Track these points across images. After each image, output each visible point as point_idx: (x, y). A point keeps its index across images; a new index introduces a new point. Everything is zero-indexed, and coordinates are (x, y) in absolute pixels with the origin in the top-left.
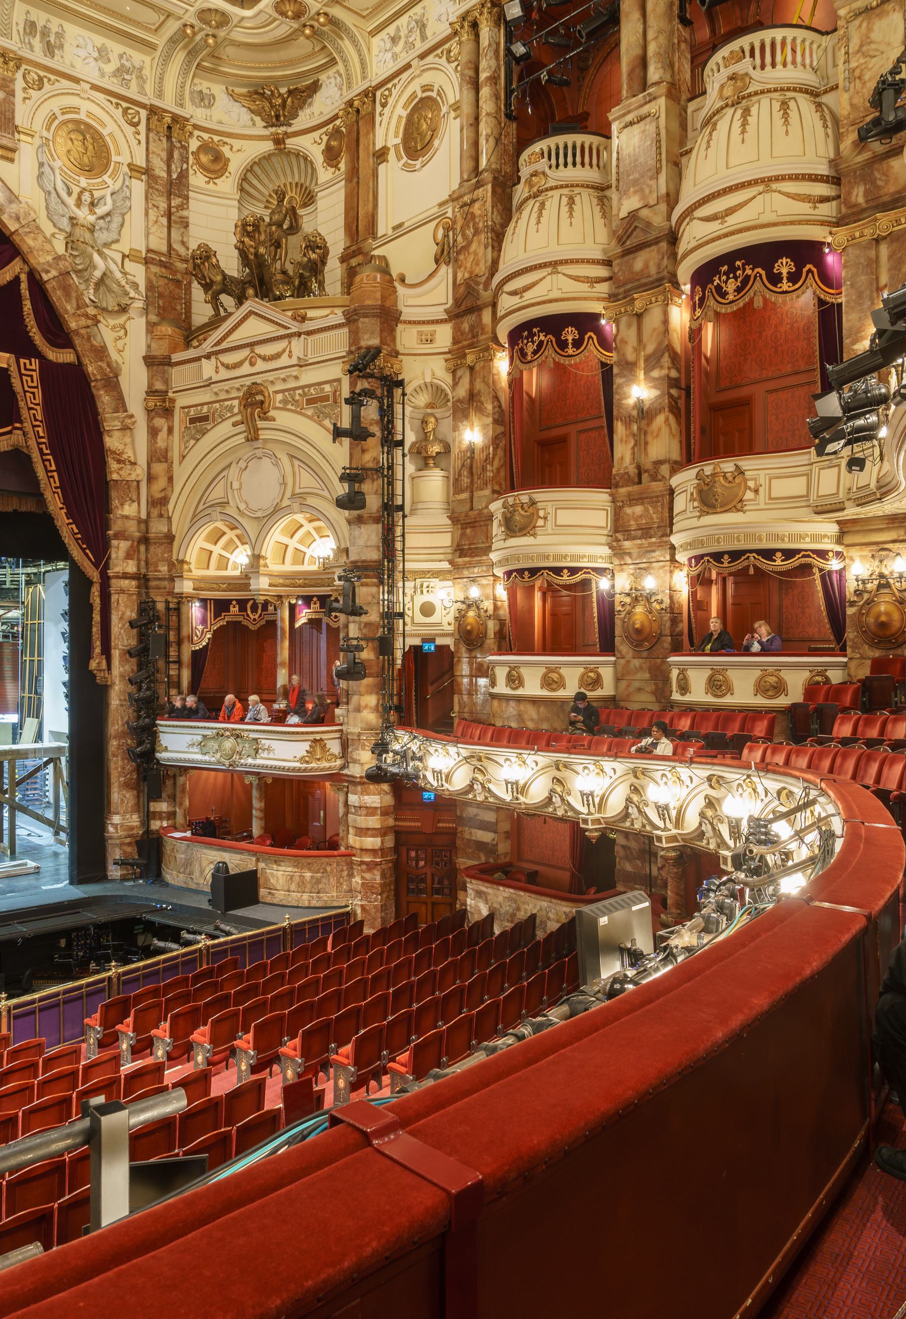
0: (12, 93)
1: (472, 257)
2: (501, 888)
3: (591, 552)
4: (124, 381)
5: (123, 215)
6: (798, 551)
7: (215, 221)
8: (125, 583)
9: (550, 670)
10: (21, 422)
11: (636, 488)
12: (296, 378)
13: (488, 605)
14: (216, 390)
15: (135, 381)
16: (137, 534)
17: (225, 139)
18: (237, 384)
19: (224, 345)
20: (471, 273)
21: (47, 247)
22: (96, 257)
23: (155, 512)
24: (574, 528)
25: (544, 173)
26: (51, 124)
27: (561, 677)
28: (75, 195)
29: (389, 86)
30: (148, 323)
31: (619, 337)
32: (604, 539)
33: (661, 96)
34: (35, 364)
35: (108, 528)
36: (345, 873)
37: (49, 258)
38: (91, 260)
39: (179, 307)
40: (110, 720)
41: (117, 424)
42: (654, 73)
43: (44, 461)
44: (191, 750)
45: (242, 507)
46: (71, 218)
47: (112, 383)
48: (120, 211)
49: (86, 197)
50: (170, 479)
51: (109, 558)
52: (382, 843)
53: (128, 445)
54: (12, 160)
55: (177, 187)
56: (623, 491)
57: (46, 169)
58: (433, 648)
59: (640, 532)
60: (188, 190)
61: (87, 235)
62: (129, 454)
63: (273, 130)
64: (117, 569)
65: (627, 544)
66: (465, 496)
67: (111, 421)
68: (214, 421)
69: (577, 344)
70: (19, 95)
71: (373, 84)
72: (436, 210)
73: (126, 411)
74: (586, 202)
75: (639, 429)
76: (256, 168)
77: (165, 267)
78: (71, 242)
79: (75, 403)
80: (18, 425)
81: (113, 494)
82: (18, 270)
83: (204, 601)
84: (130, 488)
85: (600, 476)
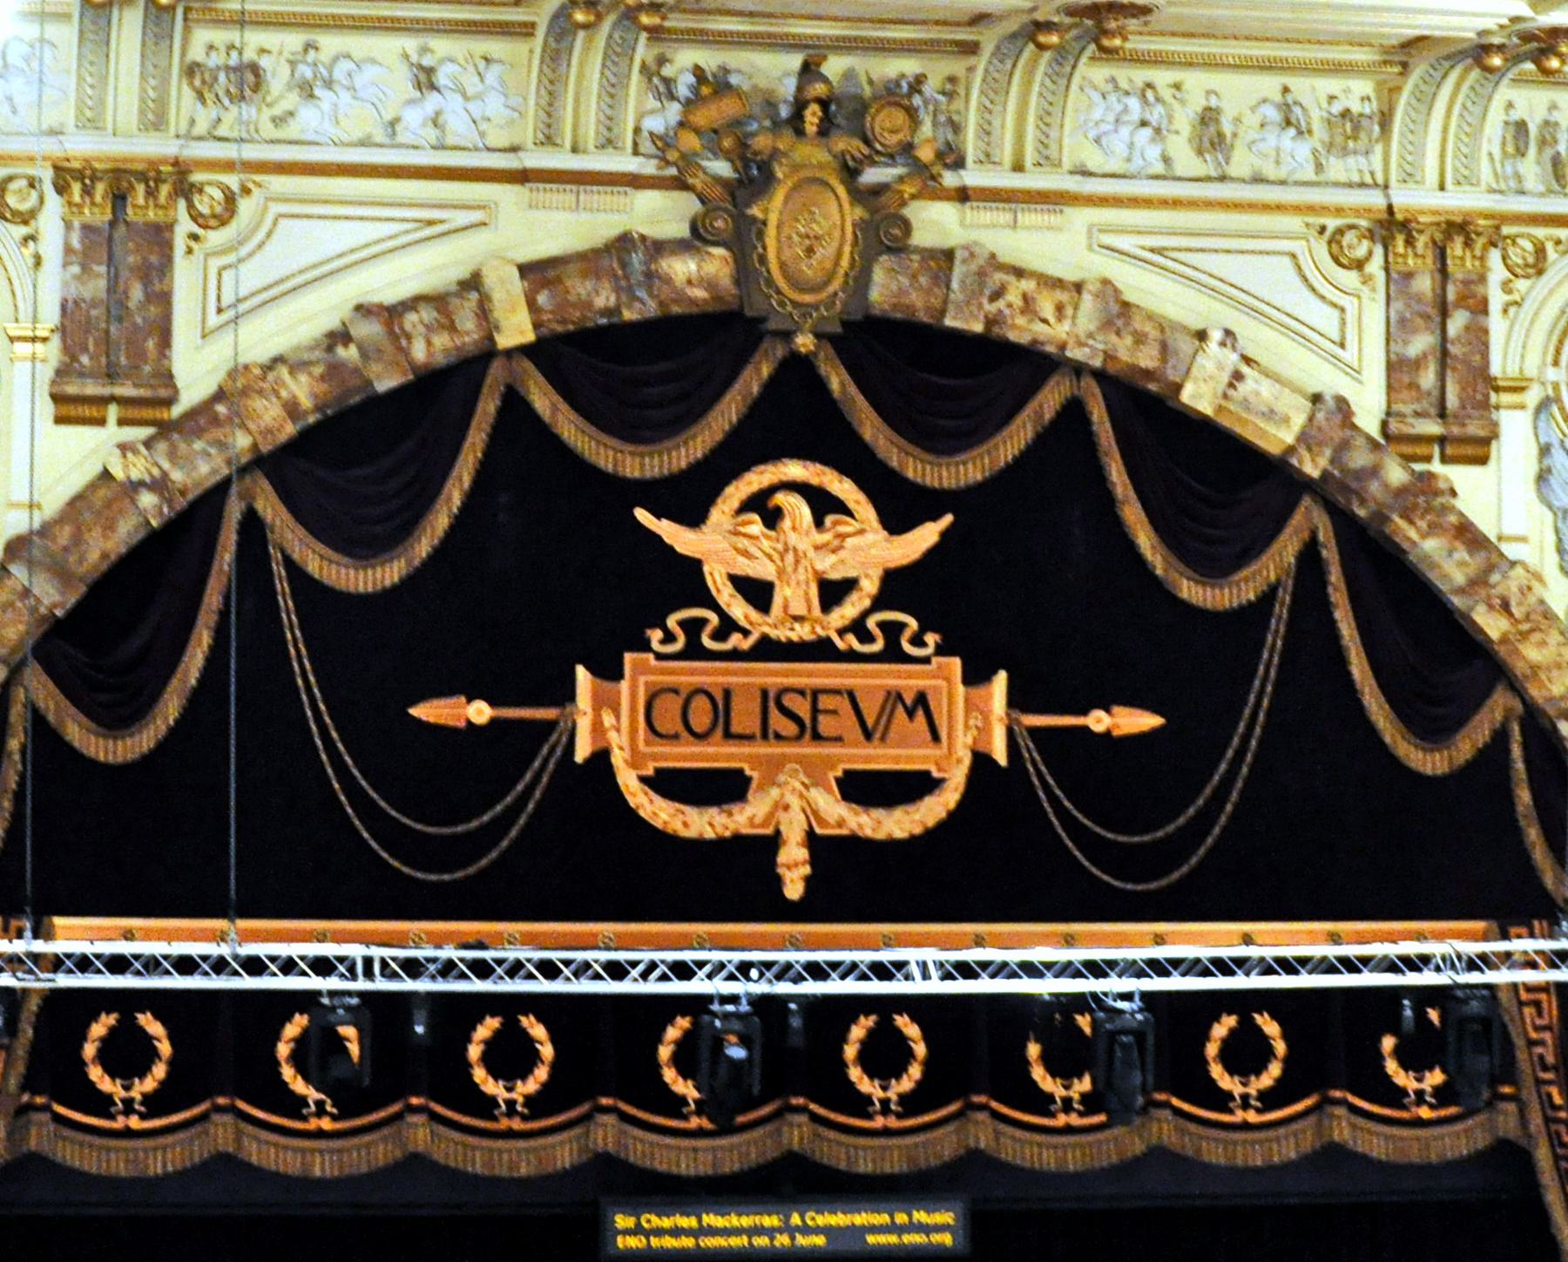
0: (1482, 308)
10: (1512, 1081)
54: (1482, 460)
70: (1496, 299)
82: (1499, 716)
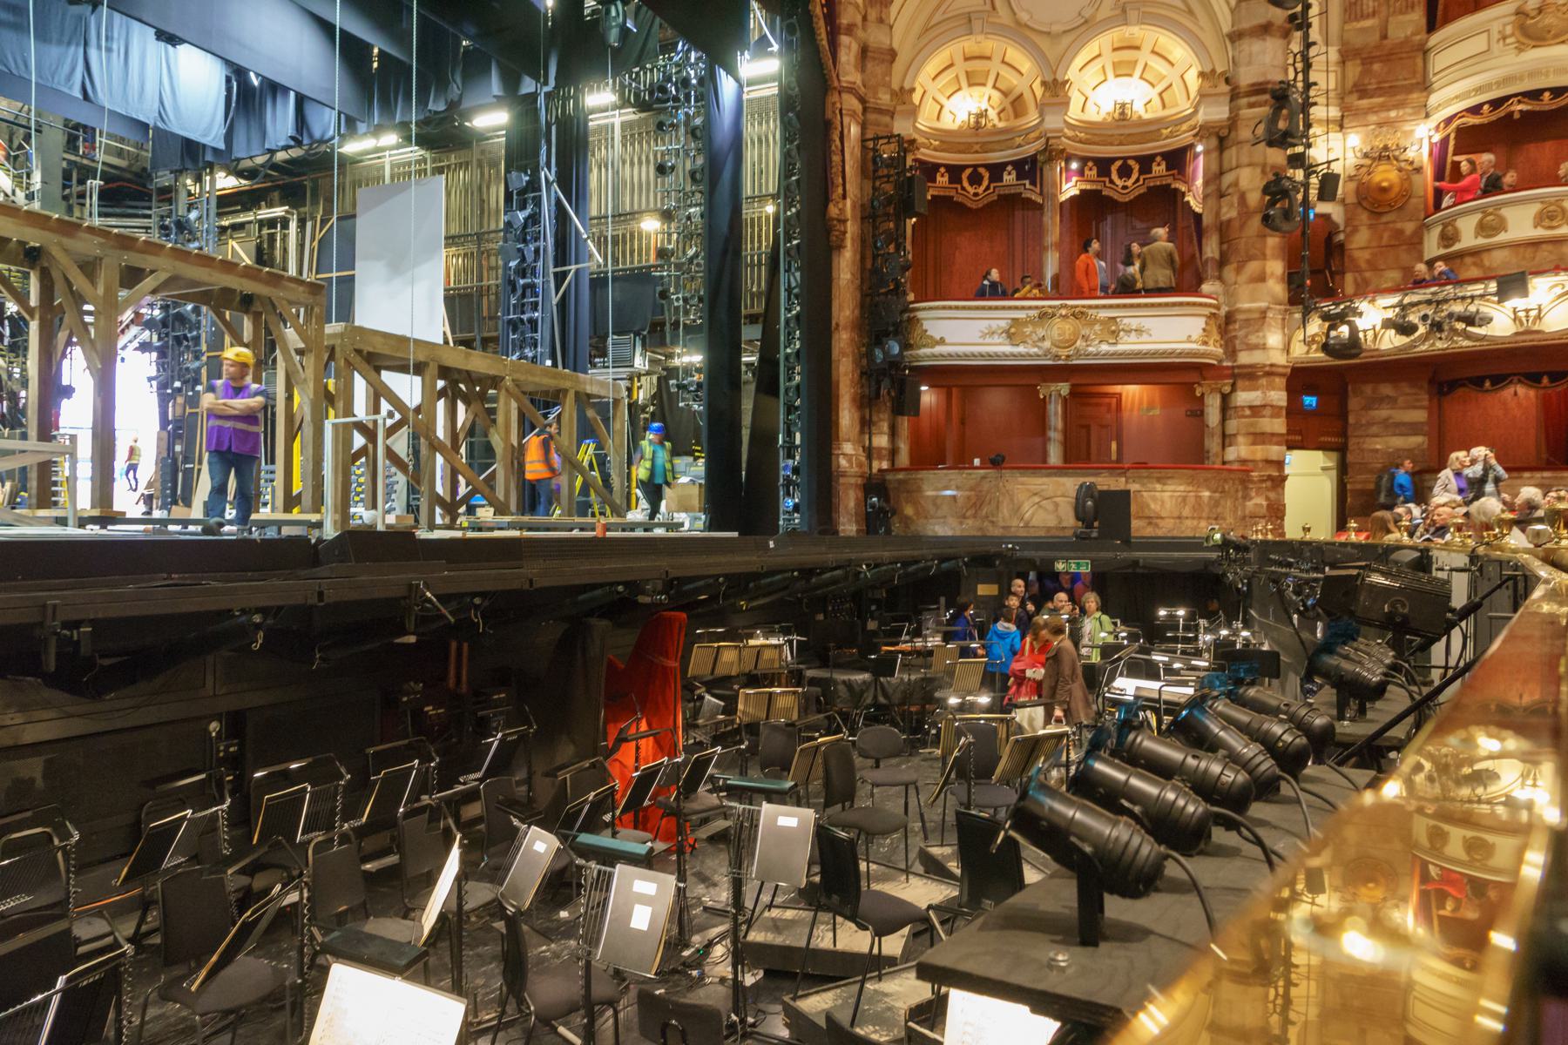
44: (988, 340)
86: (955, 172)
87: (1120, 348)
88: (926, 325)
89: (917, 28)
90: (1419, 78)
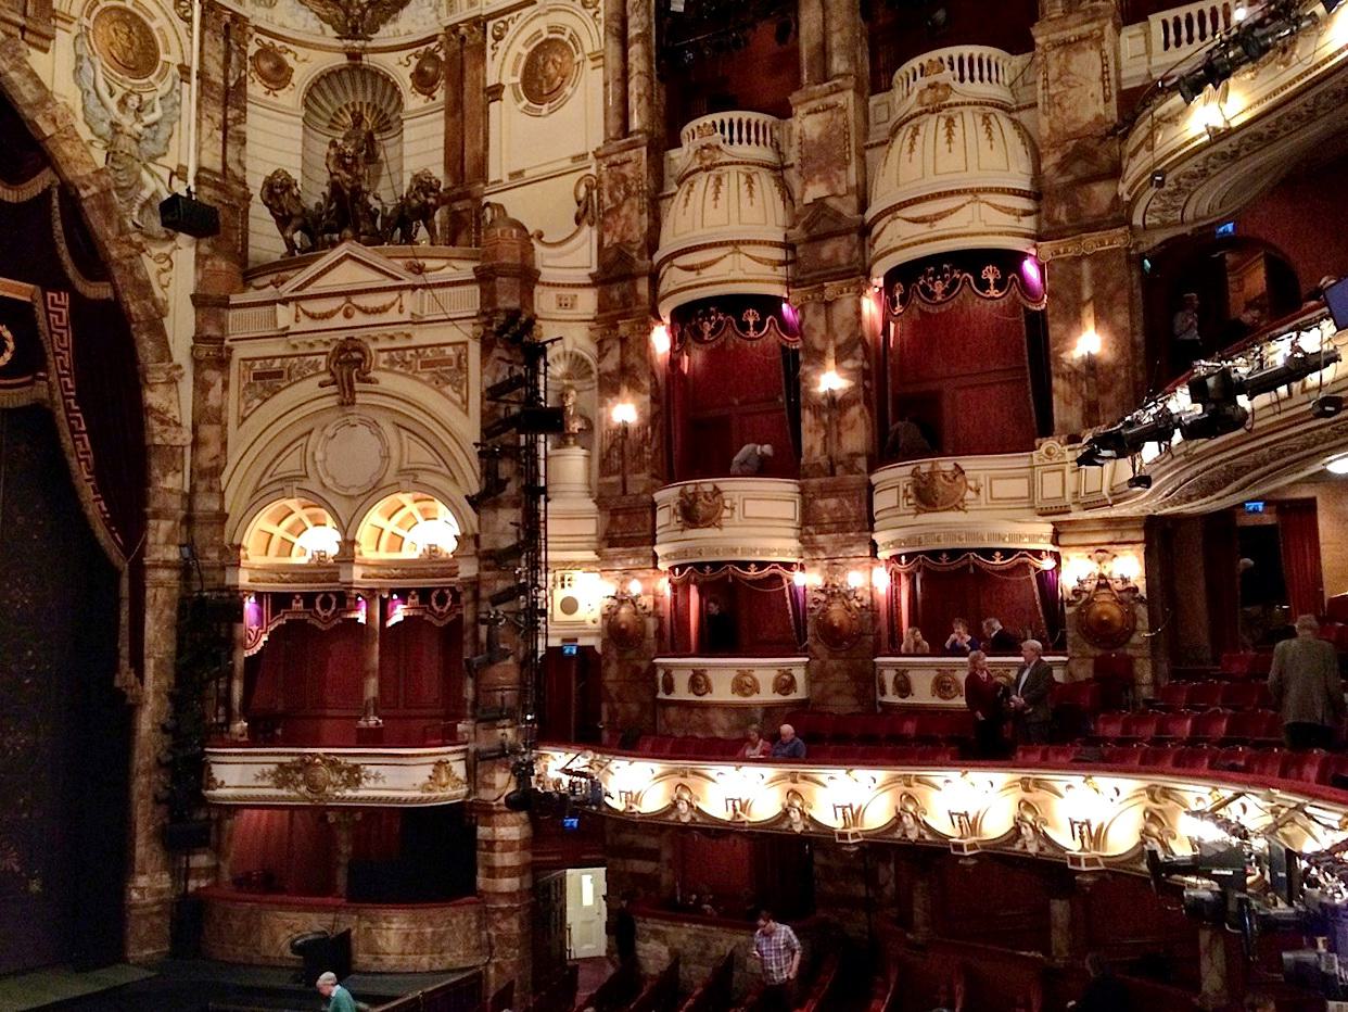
1: (623, 222)
2: (686, 925)
3: (780, 546)
4: (167, 322)
5: (172, 123)
6: (1015, 551)
7: (281, 142)
8: (163, 574)
9: (744, 674)
11: (829, 480)
12: (408, 336)
13: (647, 601)
14: (293, 342)
15: (181, 325)
16: (181, 513)
17: (289, 46)
18: (326, 337)
19: (309, 291)
20: (622, 237)
21: (87, 158)
22: (145, 175)
23: (202, 485)
24: (760, 521)
25: (718, 147)
26: (93, 9)
27: (754, 680)
28: (117, 97)
29: (505, 18)
30: (198, 255)
31: (805, 324)
32: (792, 532)
33: (849, 89)
34: (65, 299)
35: (146, 504)
36: (473, 925)
37: (89, 171)
38: (139, 177)
39: (234, 238)
40: (137, 753)
41: (162, 377)
42: (838, 64)
43: (69, 419)
45: (328, 482)
46: (114, 125)
47: (156, 328)
48: (171, 118)
49: (133, 101)
50: (224, 445)
51: (145, 542)
52: (521, 884)
53: (171, 401)
54: (46, 50)
55: (232, 97)
56: (814, 482)
57: (86, 64)
58: (574, 652)
59: (834, 526)
60: (246, 101)
61: (134, 147)
62: (174, 412)
63: (348, 42)
64: (156, 556)
65: (821, 538)
66: (614, 479)
67: (157, 375)
68: (289, 377)
69: (759, 326)
71: (484, 13)
72: (568, 163)
73: (171, 360)
74: (765, 183)
75: (829, 419)
76: (323, 83)
77: (221, 190)
78: (112, 155)
79: (112, 346)
80: (42, 374)
81: (154, 462)
82: (47, 183)
83: (259, 596)
84: (172, 453)
85: (785, 463)
86: (309, 598)
87: (361, 793)
88: (215, 768)
89: (248, 493)
90: (648, 532)
